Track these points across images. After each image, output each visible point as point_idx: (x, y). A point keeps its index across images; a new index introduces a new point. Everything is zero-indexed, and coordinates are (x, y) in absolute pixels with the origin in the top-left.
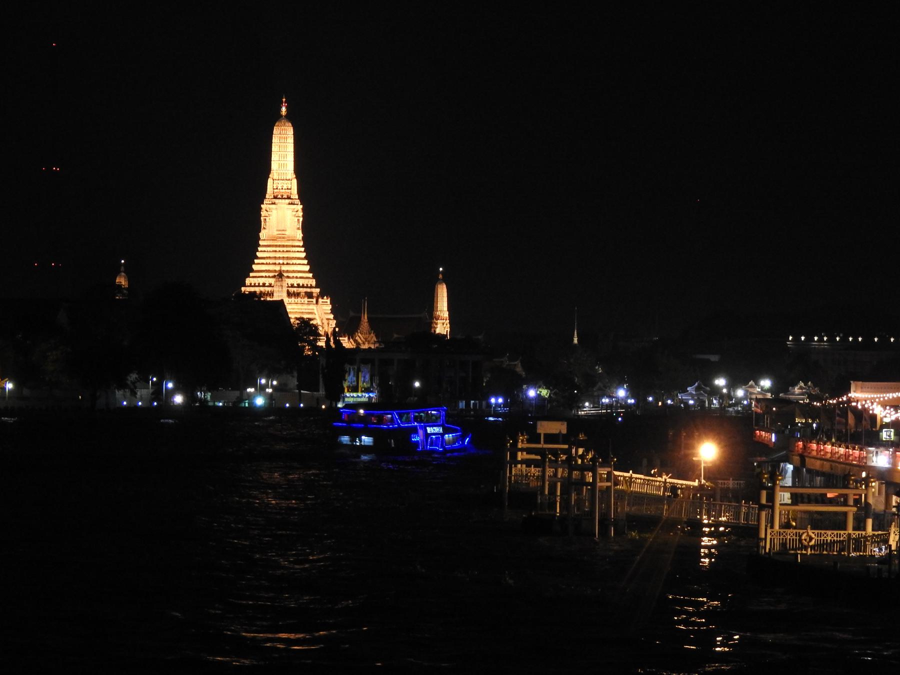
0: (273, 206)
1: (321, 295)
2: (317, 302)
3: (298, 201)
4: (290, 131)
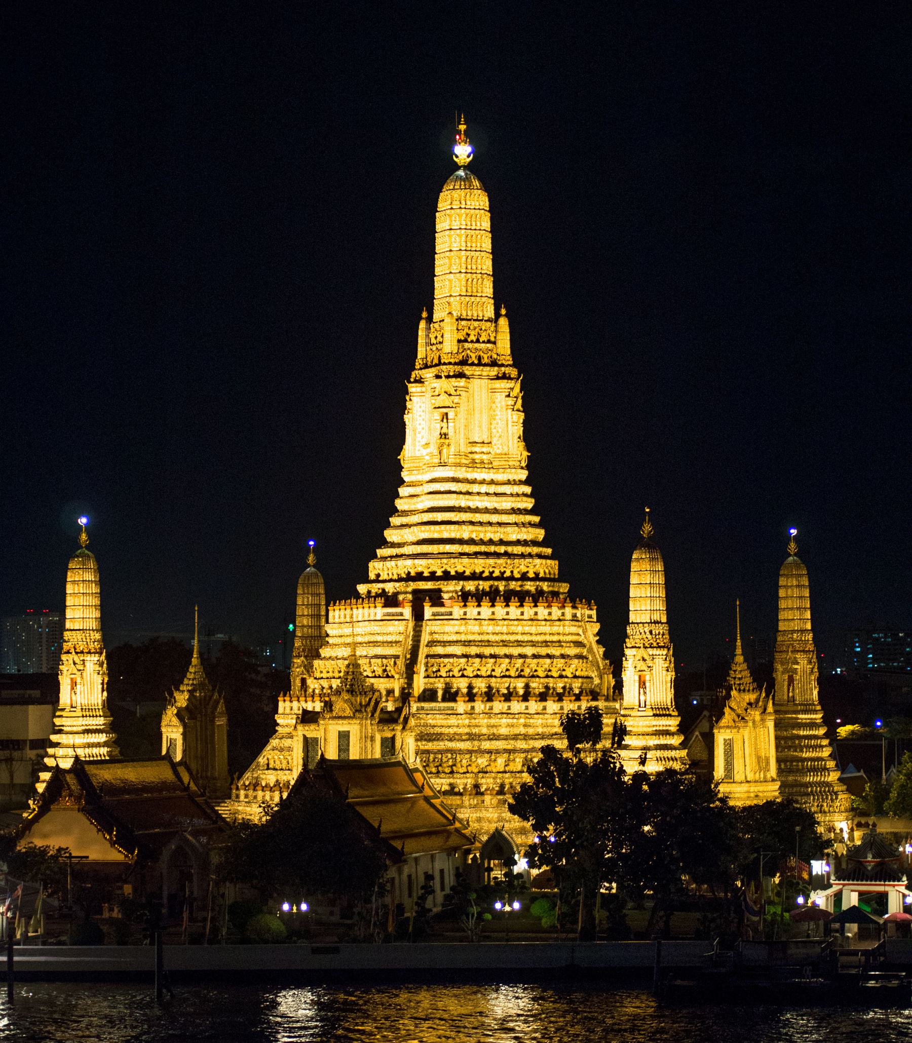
0: (462, 382)
1: (574, 598)
2: (418, 616)
3: (514, 372)
4: (480, 200)
